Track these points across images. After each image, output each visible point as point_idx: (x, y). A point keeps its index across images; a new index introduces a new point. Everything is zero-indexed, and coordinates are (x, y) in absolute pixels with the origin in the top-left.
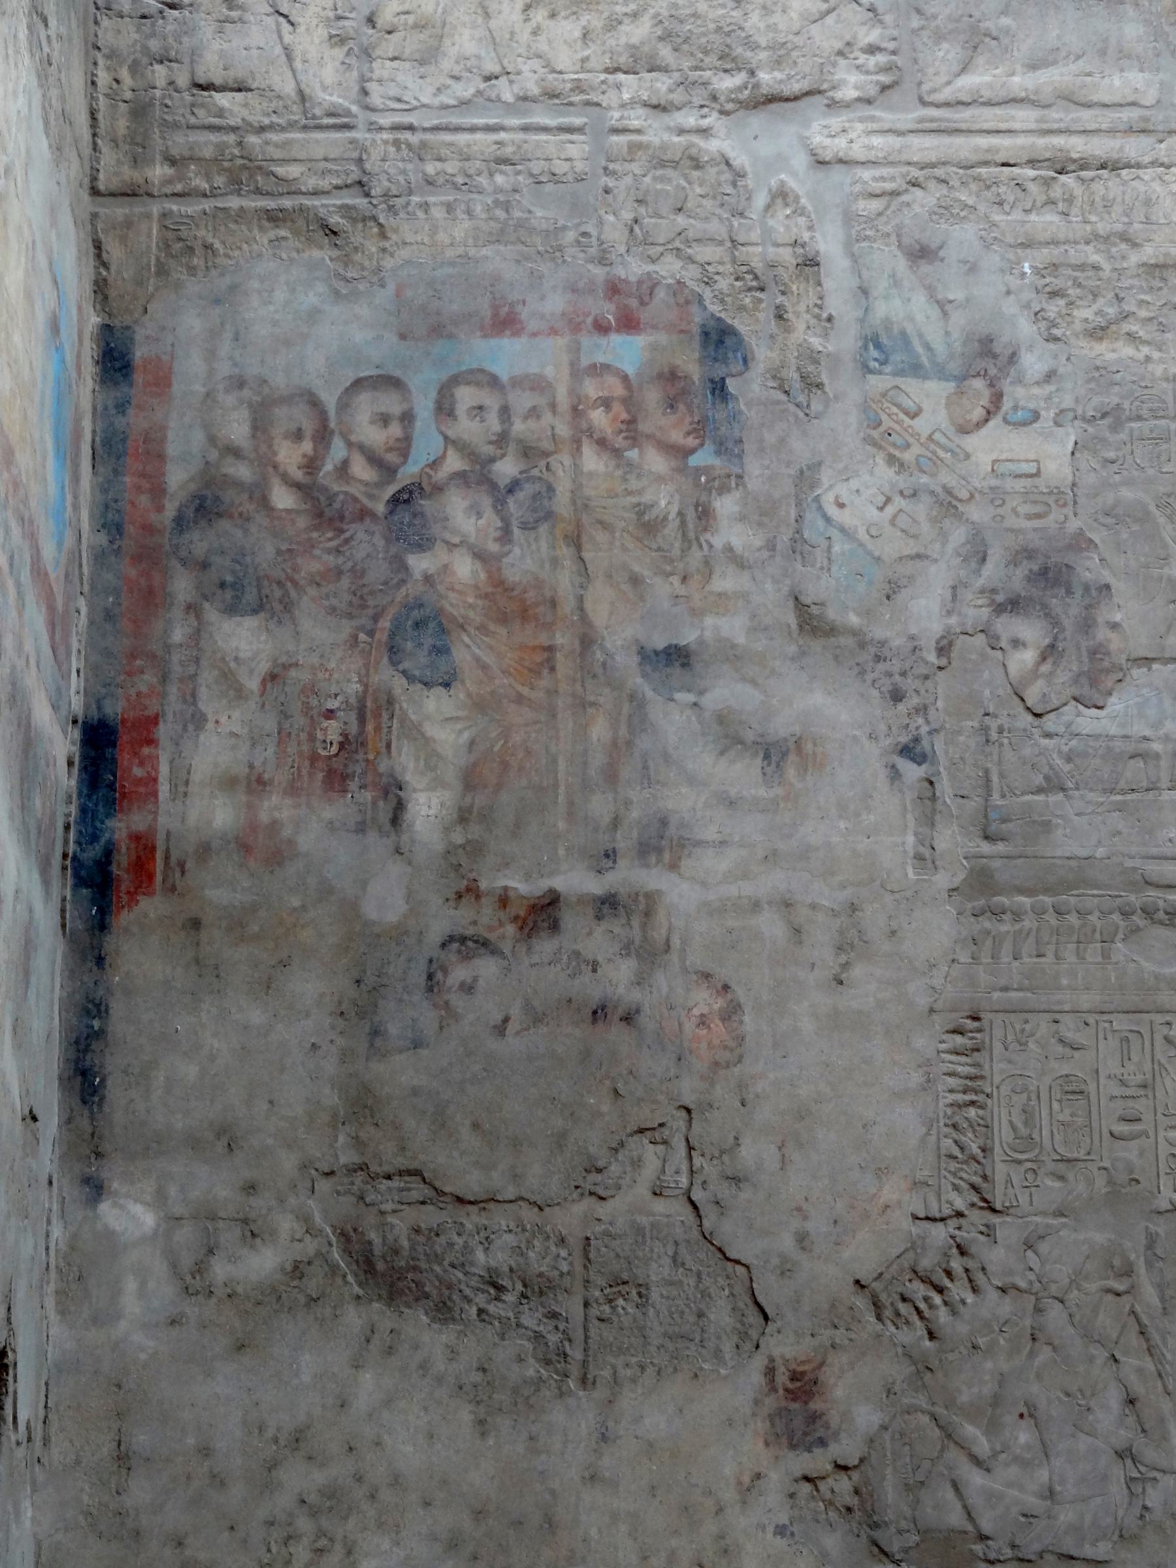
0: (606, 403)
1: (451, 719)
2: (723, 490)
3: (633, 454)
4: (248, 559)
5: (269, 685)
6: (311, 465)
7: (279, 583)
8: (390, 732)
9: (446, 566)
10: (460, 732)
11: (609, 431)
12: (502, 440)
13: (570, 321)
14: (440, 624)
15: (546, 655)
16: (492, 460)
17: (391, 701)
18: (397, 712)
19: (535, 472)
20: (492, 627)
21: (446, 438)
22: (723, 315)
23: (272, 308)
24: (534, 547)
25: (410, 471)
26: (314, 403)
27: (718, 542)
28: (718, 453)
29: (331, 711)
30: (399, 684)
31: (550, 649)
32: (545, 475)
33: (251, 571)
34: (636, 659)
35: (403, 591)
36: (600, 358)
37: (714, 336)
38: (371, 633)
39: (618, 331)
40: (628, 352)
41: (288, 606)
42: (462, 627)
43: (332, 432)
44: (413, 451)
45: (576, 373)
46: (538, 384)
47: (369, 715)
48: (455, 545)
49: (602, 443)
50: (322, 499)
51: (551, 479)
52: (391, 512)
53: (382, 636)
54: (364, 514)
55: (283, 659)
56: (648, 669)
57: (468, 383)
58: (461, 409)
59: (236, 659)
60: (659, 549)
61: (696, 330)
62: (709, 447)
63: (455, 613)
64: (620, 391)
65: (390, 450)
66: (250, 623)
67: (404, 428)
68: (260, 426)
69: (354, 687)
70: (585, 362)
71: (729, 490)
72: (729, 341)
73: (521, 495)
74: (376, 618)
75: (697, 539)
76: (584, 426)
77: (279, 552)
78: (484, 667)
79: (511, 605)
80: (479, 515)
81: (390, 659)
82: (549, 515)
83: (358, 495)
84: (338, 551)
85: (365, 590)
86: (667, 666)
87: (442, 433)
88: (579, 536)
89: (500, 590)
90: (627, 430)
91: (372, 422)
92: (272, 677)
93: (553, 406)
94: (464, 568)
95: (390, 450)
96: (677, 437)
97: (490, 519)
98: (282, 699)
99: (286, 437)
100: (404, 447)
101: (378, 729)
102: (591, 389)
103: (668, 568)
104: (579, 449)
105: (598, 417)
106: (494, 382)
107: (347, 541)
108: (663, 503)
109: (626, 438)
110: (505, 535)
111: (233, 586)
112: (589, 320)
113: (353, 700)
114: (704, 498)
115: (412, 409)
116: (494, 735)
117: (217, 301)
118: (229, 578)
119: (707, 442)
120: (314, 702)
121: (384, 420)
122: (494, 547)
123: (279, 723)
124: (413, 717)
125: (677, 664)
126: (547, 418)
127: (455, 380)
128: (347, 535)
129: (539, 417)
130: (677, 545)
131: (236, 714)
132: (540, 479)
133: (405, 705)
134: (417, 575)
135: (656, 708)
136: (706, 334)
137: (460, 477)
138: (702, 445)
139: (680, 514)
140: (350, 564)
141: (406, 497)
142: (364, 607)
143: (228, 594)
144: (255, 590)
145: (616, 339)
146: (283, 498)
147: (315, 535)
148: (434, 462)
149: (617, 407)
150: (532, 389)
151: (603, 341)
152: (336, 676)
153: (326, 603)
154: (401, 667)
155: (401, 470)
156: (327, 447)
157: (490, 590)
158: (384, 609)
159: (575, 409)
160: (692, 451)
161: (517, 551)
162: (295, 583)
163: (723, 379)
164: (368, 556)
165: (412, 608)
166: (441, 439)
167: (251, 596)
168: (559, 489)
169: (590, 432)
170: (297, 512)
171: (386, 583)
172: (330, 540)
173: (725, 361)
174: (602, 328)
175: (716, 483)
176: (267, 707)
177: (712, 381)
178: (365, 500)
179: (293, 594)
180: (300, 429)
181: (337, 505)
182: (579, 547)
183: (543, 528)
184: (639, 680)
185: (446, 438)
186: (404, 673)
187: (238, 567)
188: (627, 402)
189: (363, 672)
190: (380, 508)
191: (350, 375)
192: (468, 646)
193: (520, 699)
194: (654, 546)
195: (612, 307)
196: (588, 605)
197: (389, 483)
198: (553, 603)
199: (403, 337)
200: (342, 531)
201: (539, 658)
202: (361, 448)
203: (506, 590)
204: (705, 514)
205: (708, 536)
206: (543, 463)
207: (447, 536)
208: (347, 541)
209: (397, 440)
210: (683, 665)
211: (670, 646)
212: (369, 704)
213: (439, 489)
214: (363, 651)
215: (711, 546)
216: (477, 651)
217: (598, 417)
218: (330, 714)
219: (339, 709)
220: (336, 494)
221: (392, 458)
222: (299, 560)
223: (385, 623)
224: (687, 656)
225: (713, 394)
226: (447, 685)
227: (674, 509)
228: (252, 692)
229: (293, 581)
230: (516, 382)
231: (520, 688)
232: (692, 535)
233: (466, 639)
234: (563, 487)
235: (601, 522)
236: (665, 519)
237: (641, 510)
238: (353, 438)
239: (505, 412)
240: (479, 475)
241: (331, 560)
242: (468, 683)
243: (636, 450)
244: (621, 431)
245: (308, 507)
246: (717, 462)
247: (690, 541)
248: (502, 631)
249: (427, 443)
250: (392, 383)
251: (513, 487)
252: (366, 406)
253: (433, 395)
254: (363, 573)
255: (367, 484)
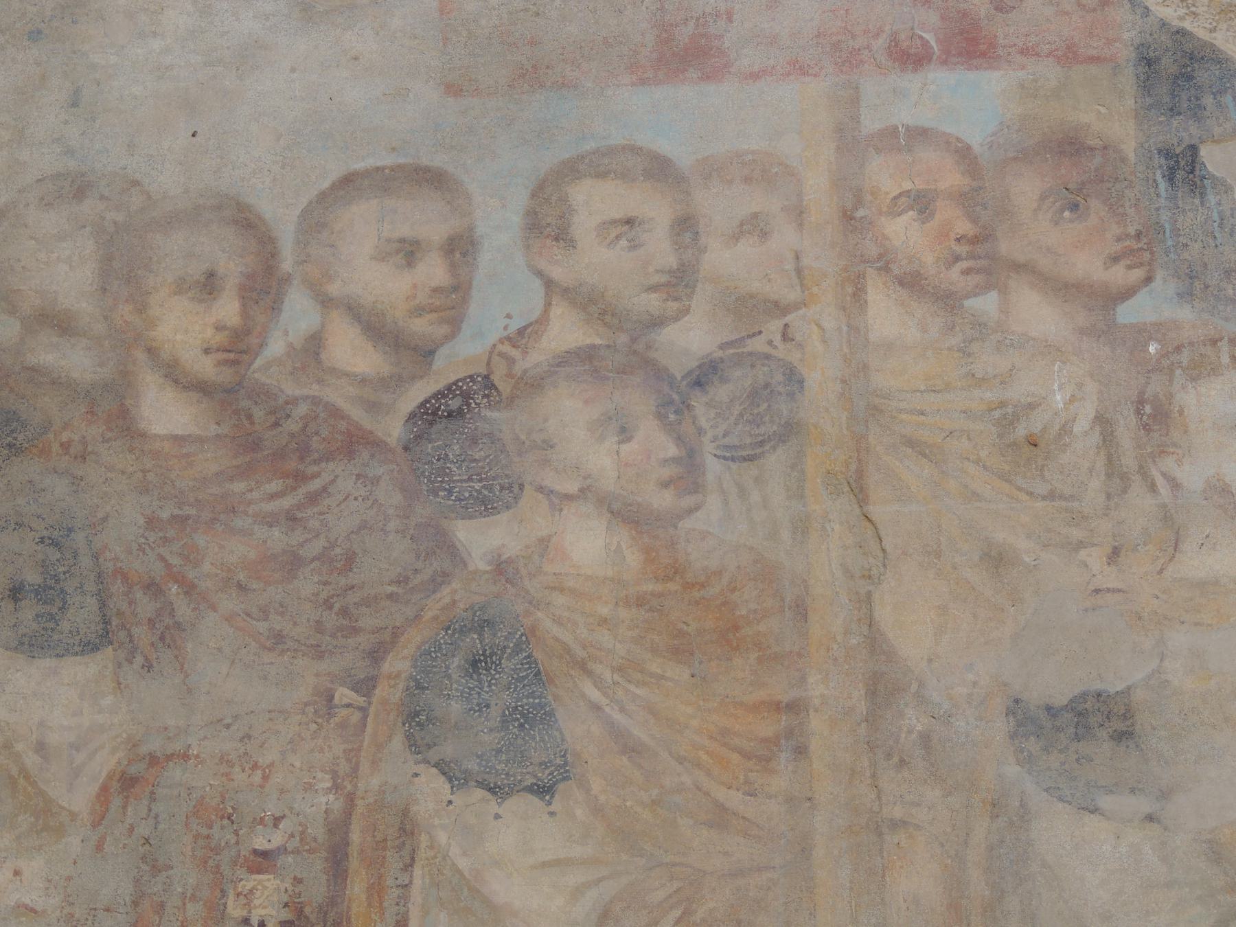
0: (922, 203)
1: (557, 863)
2: (1200, 370)
3: (986, 304)
4: (79, 538)
5: (117, 802)
6: (238, 347)
7: (153, 588)
8: (404, 899)
9: (544, 542)
10: (577, 892)
11: (929, 259)
12: (680, 282)
13: (836, 46)
14: (530, 660)
15: (784, 720)
16: (657, 322)
17: (407, 829)
18: (422, 854)
19: (757, 345)
20: (654, 667)
21: (549, 284)
22: (1187, 25)
23: (156, 44)
24: (755, 497)
25: (461, 355)
26: (247, 221)
27: (1193, 476)
28: (1186, 296)
29: (265, 854)
30: (430, 788)
31: (794, 707)
32: (781, 351)
33: (86, 561)
34: (1001, 727)
35: (445, 594)
36: (904, 115)
37: (1168, 65)
38: (365, 686)
39: (945, 62)
40: (973, 104)
41: (170, 634)
42: (583, 667)
43: (286, 280)
44: (473, 309)
45: (850, 143)
46: (762, 171)
47: (354, 863)
48: (568, 497)
49: (912, 283)
50: (258, 413)
51: (794, 357)
52: (418, 437)
53: (389, 692)
54: (354, 442)
55: (155, 745)
56: (1033, 745)
57: (602, 175)
58: (584, 225)
59: (41, 747)
60: (1052, 496)
61: (1125, 54)
62: (1164, 286)
63: (567, 637)
64: (953, 178)
65: (419, 311)
66: (82, 670)
67: (453, 267)
68: (123, 269)
69: (320, 803)
70: (870, 123)
71: (1215, 371)
72: (1203, 76)
73: (722, 392)
74: (376, 655)
75: (1143, 472)
76: (872, 250)
77: (152, 522)
78: (632, 749)
79: (705, 619)
80: (625, 434)
81: (409, 737)
82: (790, 430)
83: (341, 403)
84: (292, 519)
85: (353, 598)
86: (1078, 738)
87: (539, 273)
88: (860, 474)
89: (673, 586)
90: (972, 256)
91: (381, 256)
92: (127, 782)
93: (798, 214)
94: (588, 544)
95: (419, 311)
96: (1088, 265)
97: (654, 443)
98: (144, 829)
99: (181, 287)
100: (452, 303)
101: (376, 890)
102: (885, 176)
103: (1076, 534)
104: (859, 293)
105: (903, 232)
106: (659, 170)
107: (313, 498)
108: (1059, 399)
109: (967, 272)
110: (687, 475)
111: (40, 592)
112: (880, 43)
113: (317, 830)
114: (1156, 387)
115: (471, 229)
116: (660, 895)
117: (35, 35)
118: (32, 577)
119: (1160, 275)
120: (222, 834)
121: (409, 252)
122: (663, 500)
123: (137, 881)
124: (463, 864)
125: (1103, 734)
126: (785, 237)
127: (571, 170)
128: (316, 485)
129: (764, 235)
130: (1095, 484)
131: (34, 867)
132: (768, 357)
133: (442, 837)
134: (479, 562)
135: (1057, 831)
136: (1147, 61)
137: (587, 355)
138: (1148, 280)
139: (1102, 421)
140: (320, 543)
141: (455, 404)
142: (355, 631)
143: (29, 611)
144: (92, 603)
145: (939, 78)
146: (165, 413)
147: (239, 486)
148: (521, 332)
149: (946, 212)
150: (747, 180)
151: (911, 82)
152: (277, 779)
153: (262, 626)
154: (433, 755)
155: (443, 352)
156: (275, 308)
157: (650, 587)
158: (396, 634)
159: (847, 217)
160: (1127, 293)
161: (713, 502)
162: (189, 589)
163: (1193, 149)
164: (364, 526)
165: (463, 631)
166: (537, 284)
167: (82, 614)
168: (813, 379)
169: (884, 263)
170: (201, 440)
171: (402, 580)
172: (272, 497)
173: (1197, 112)
174: (911, 58)
175: (1185, 357)
176: (108, 848)
177: (1166, 153)
178: (357, 413)
179: (183, 610)
180: (211, 275)
181: (292, 426)
182: (860, 493)
183: (776, 460)
184: (1012, 770)
185: (549, 284)
186: (443, 768)
187: (54, 555)
188: (967, 200)
189: (344, 767)
190: (394, 429)
191: (335, 171)
192: (597, 708)
193: (721, 817)
194: (1042, 489)
195: (933, 18)
196: (884, 613)
197: (413, 378)
198: (801, 611)
199: (452, 90)
200: (300, 478)
201: (767, 728)
202: (353, 309)
203: (688, 586)
204: (1157, 418)
205: (1169, 464)
206: (774, 327)
207: (550, 479)
208: (313, 498)
209: (436, 290)
210: (1121, 736)
211: (1084, 696)
212: (355, 837)
213: (532, 385)
214: (343, 725)
215: (1175, 485)
216: (618, 717)
217: (903, 232)
218: (263, 860)
219: (283, 850)
220: (294, 402)
221: (421, 326)
222: (201, 540)
223: (398, 664)
224: (1127, 715)
225: (1171, 179)
226: (543, 791)
227: (1086, 413)
228: (73, 816)
229: (180, 580)
230: (711, 170)
231: (721, 794)
232: (1129, 461)
233: (594, 694)
234: (822, 374)
235: (910, 443)
236: (1065, 430)
237: (1007, 417)
238: (334, 289)
239: (686, 226)
240: (622, 352)
241: (277, 538)
242: (596, 785)
243: (993, 296)
244: (957, 259)
245: (224, 429)
246: (1185, 314)
247: (1124, 477)
248: (678, 673)
249: (503, 297)
250: (431, 179)
251: (705, 375)
252: (364, 226)
253: (519, 199)
254: (350, 560)
255: (364, 381)
